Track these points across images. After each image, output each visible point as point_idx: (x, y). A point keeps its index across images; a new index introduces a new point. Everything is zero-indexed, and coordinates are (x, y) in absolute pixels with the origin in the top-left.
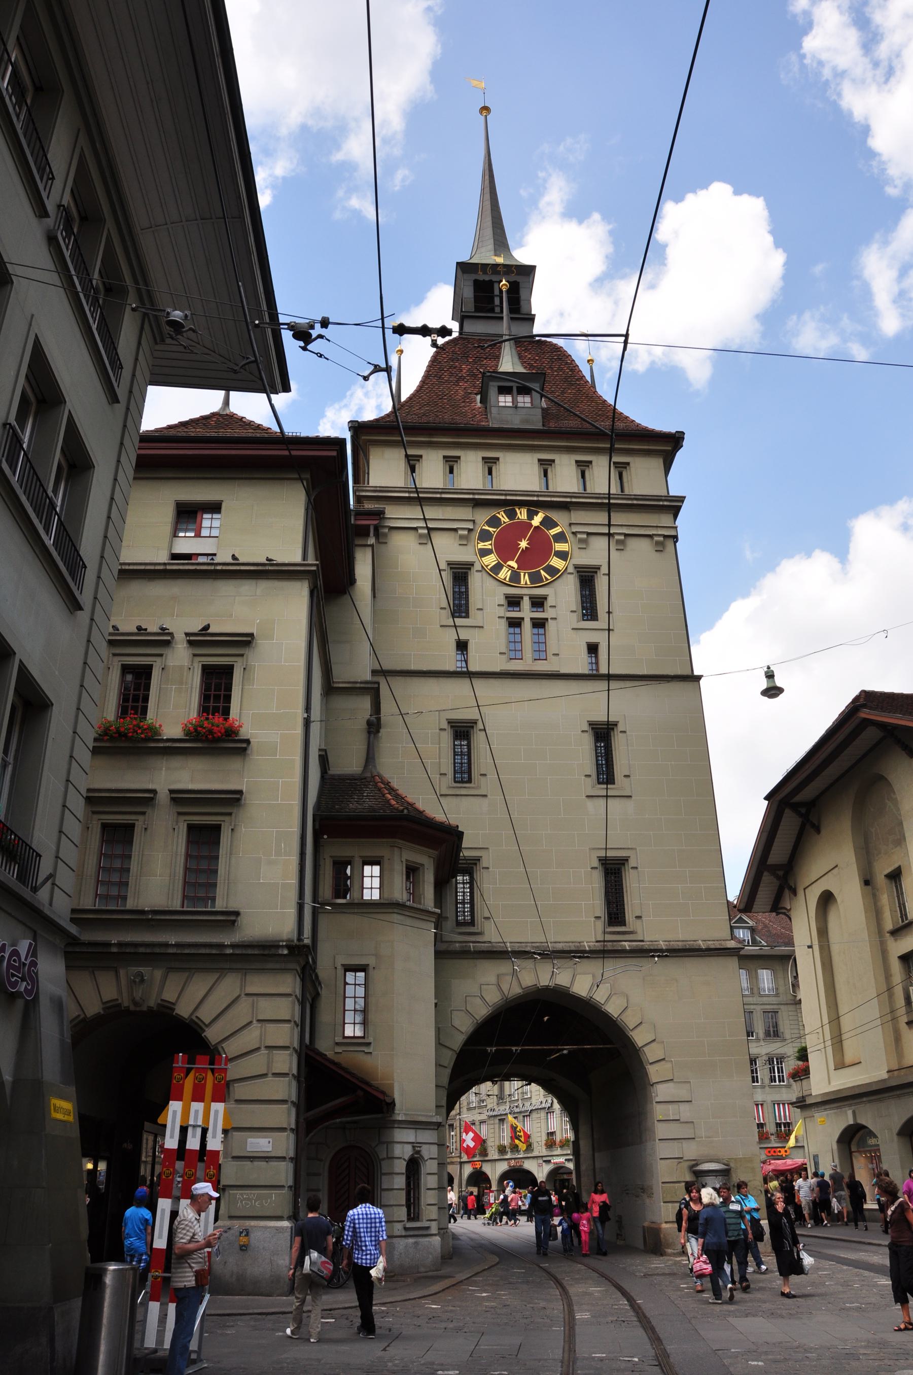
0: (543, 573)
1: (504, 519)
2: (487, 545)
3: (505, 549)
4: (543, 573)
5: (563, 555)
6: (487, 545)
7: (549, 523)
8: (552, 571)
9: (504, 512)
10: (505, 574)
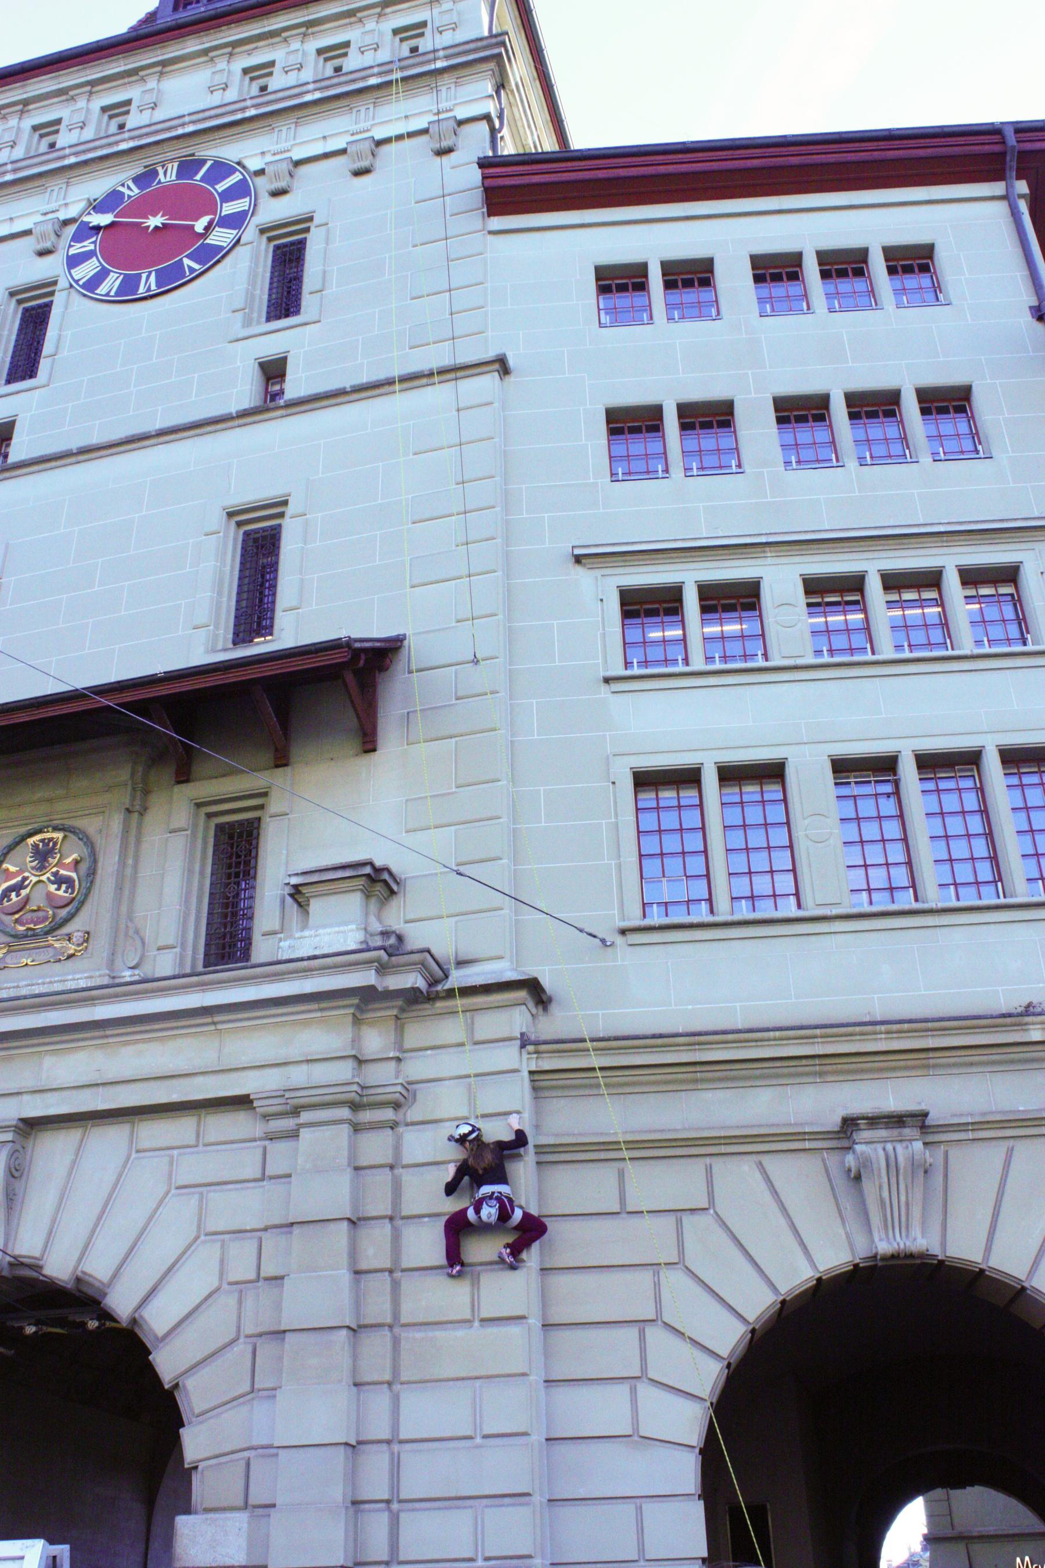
0: (187, 262)
4: (187, 262)
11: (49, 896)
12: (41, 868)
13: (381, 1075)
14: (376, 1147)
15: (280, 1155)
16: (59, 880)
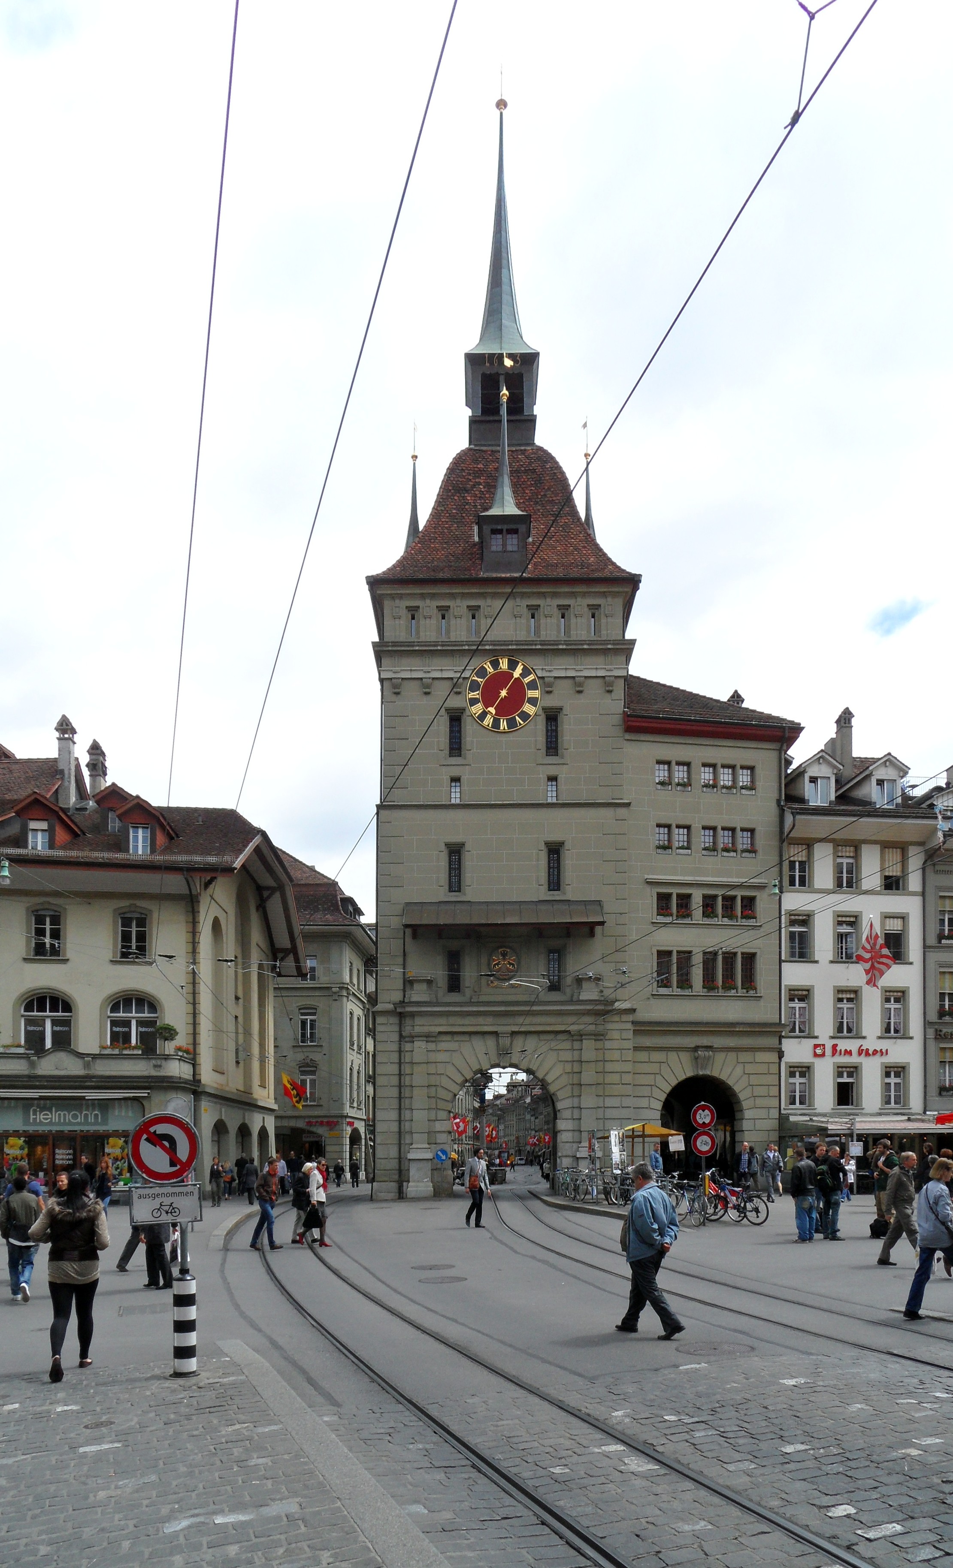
0: (517, 718)
1: (490, 669)
2: (475, 695)
3: (489, 698)
4: (517, 718)
5: (533, 701)
6: (475, 695)
7: (526, 672)
8: (525, 716)
9: (490, 662)
10: (488, 721)
11: (508, 969)
12: (504, 959)
13: (600, 1028)
14: (599, 1045)
15: (577, 1045)
16: (510, 964)
